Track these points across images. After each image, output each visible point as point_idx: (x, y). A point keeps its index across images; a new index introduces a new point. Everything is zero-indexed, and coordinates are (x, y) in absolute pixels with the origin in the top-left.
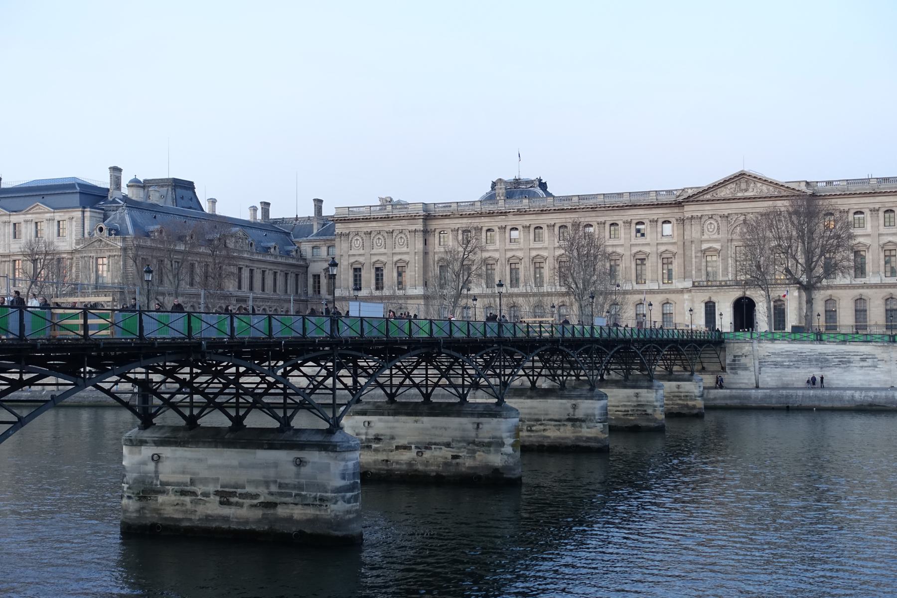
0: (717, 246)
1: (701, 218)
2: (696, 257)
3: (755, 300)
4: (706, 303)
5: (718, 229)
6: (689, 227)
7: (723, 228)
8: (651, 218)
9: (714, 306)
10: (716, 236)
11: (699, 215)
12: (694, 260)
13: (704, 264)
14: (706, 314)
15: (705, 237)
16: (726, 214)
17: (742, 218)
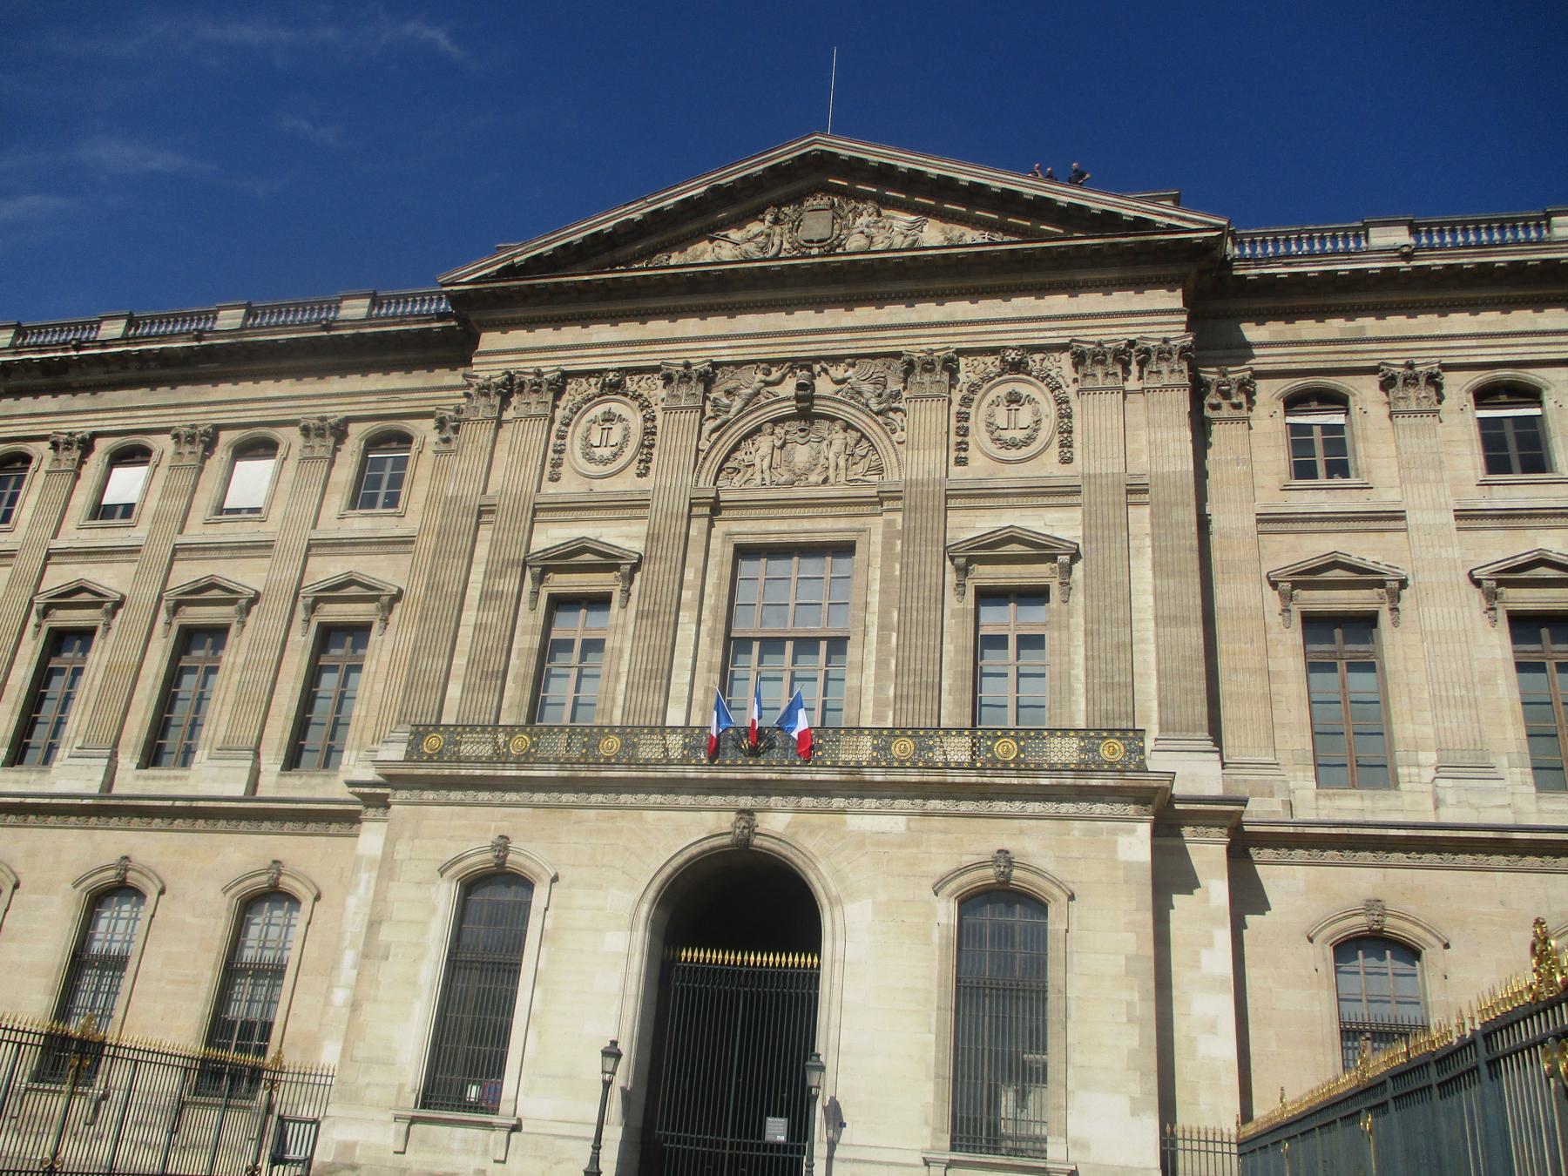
0: (624, 536)
1: (558, 386)
2: (487, 597)
3: (824, 878)
4: (472, 885)
5: (647, 446)
6: (484, 434)
7: (679, 435)
8: (309, 413)
9: (524, 909)
10: (627, 483)
11: (549, 367)
12: (469, 616)
13: (526, 641)
14: (454, 963)
15: (569, 486)
16: (698, 358)
17: (788, 388)
